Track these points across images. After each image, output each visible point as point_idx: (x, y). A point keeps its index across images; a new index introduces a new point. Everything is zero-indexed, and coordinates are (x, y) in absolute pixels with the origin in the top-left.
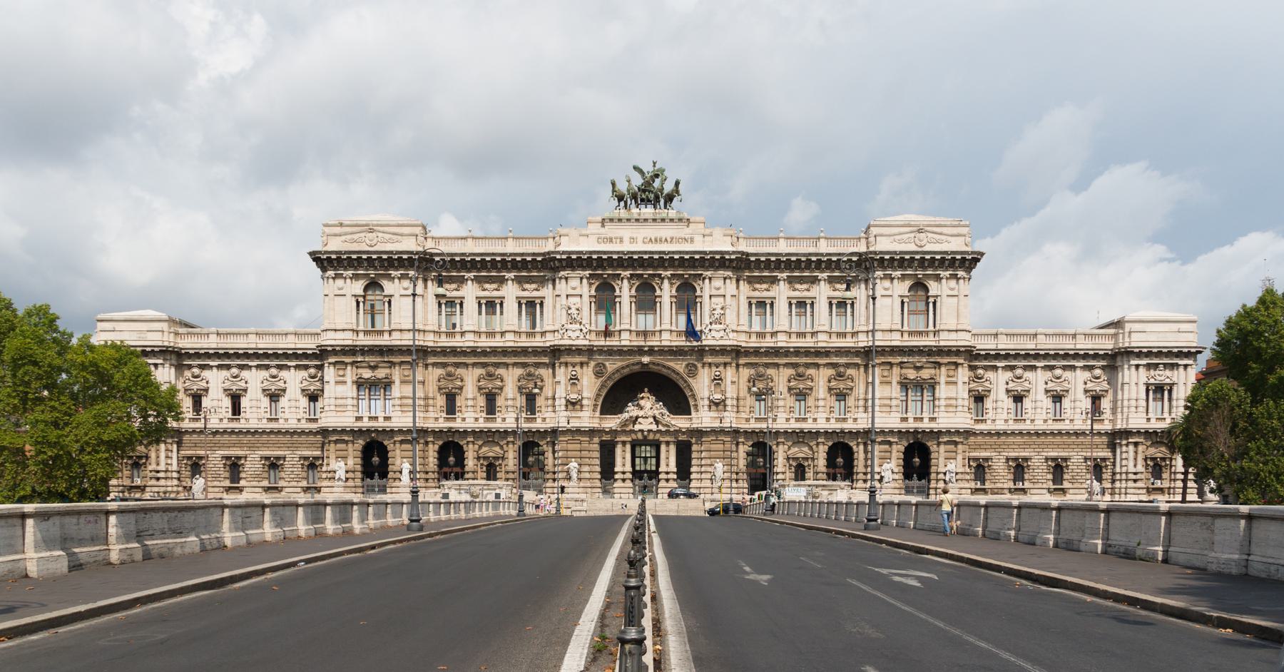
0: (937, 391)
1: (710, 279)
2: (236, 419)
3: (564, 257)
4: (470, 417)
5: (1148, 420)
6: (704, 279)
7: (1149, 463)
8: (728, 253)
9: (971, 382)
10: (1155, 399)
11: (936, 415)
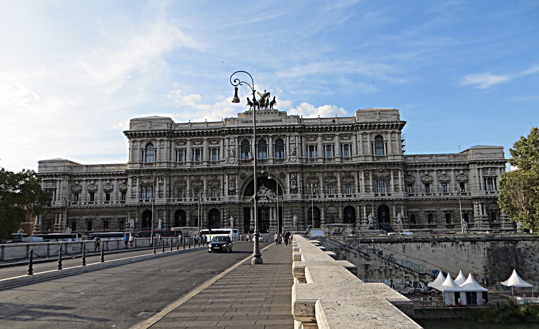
0: (390, 182)
1: (289, 137)
2: (92, 202)
3: (227, 129)
4: (188, 200)
5: (487, 193)
6: (287, 136)
7: (490, 212)
8: (296, 125)
9: (406, 178)
10: (489, 183)
11: (390, 193)
